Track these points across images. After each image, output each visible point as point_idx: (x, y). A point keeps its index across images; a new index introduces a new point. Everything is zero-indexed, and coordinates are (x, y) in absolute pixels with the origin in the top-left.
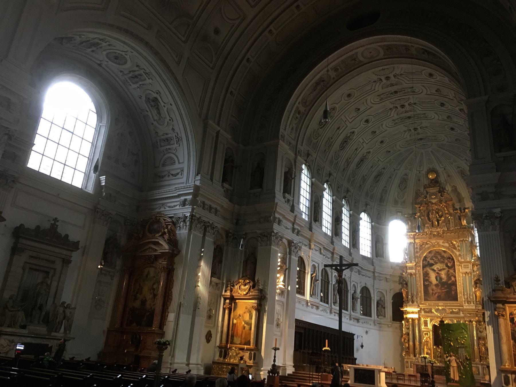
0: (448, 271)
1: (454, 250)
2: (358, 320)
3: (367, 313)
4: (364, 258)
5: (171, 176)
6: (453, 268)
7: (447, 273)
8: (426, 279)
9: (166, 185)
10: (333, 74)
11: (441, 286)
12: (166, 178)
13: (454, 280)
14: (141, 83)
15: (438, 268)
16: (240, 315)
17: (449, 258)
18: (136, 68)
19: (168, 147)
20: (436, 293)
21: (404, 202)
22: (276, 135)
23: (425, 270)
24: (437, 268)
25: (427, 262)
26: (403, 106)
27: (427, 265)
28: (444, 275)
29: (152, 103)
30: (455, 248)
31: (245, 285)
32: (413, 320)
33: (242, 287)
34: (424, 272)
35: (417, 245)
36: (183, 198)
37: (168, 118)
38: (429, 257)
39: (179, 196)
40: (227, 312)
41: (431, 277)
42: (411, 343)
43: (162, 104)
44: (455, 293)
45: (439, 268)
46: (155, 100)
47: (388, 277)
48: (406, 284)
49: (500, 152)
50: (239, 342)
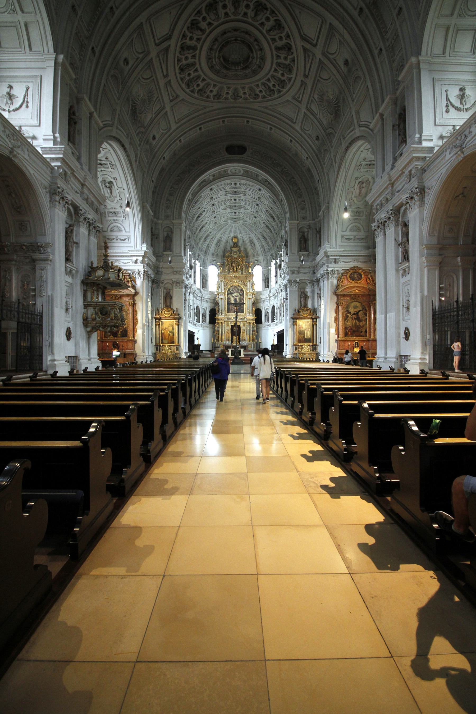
2: (195, 325)
3: (198, 321)
4: (198, 289)
5: (119, 241)
9: (115, 246)
10: (211, 178)
12: (115, 241)
14: (103, 169)
16: (166, 328)
17: (241, 290)
18: (104, 159)
19: (115, 218)
21: (217, 255)
22: (180, 217)
26: (235, 200)
27: (230, 293)
29: (107, 185)
30: (245, 285)
31: (168, 311)
32: (222, 323)
33: (166, 312)
36: (135, 258)
37: (118, 198)
39: (131, 256)
40: (158, 326)
42: (220, 335)
43: (116, 187)
46: (111, 183)
47: (208, 300)
48: (218, 304)
49: (300, 251)
50: (167, 342)
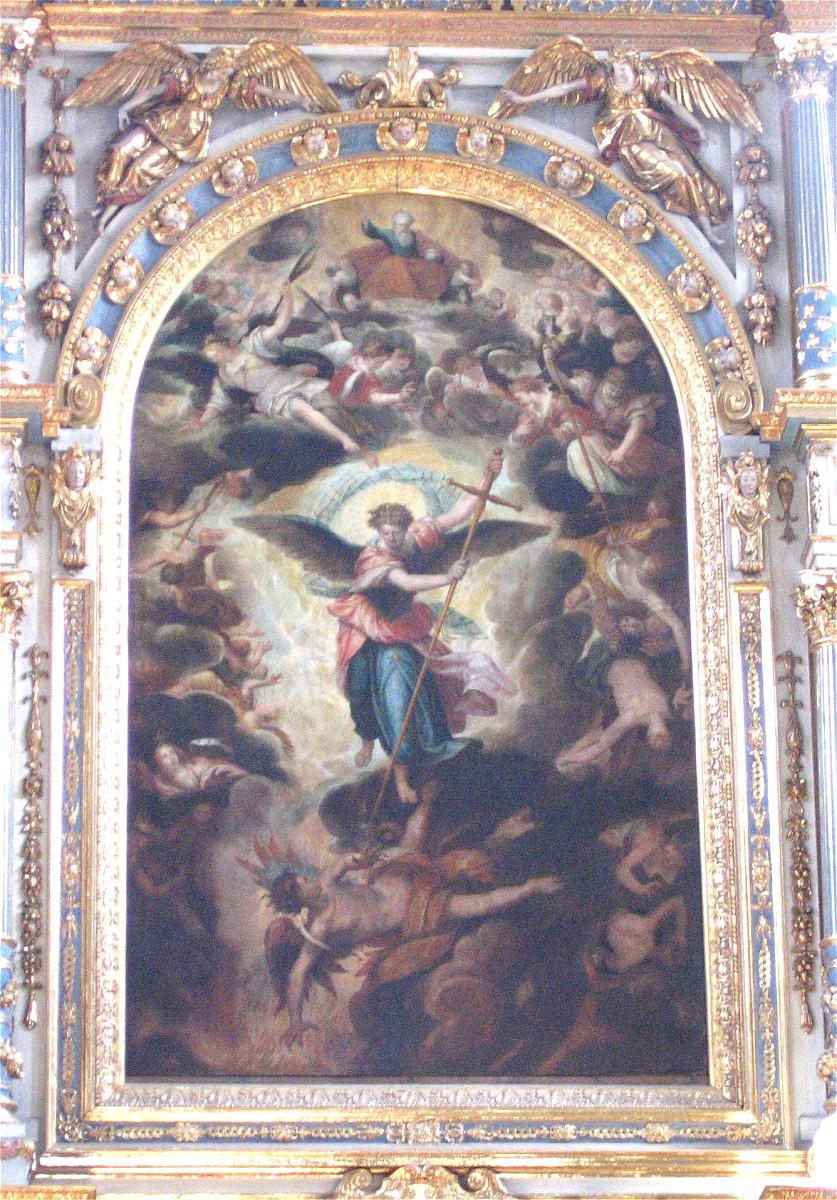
0: (569, 570)
1: (683, 224)
6: (641, 517)
7: (552, 605)
8: (177, 691)
11: (431, 824)
13: (657, 728)
15: (404, 518)
20: (339, 944)
23: (170, 546)
24: (377, 518)
25: (218, 399)
28: (489, 627)
34: (153, 576)
35: (57, 105)
38: (260, 321)
41: (273, 662)
44: (659, 936)
45: (419, 509)
